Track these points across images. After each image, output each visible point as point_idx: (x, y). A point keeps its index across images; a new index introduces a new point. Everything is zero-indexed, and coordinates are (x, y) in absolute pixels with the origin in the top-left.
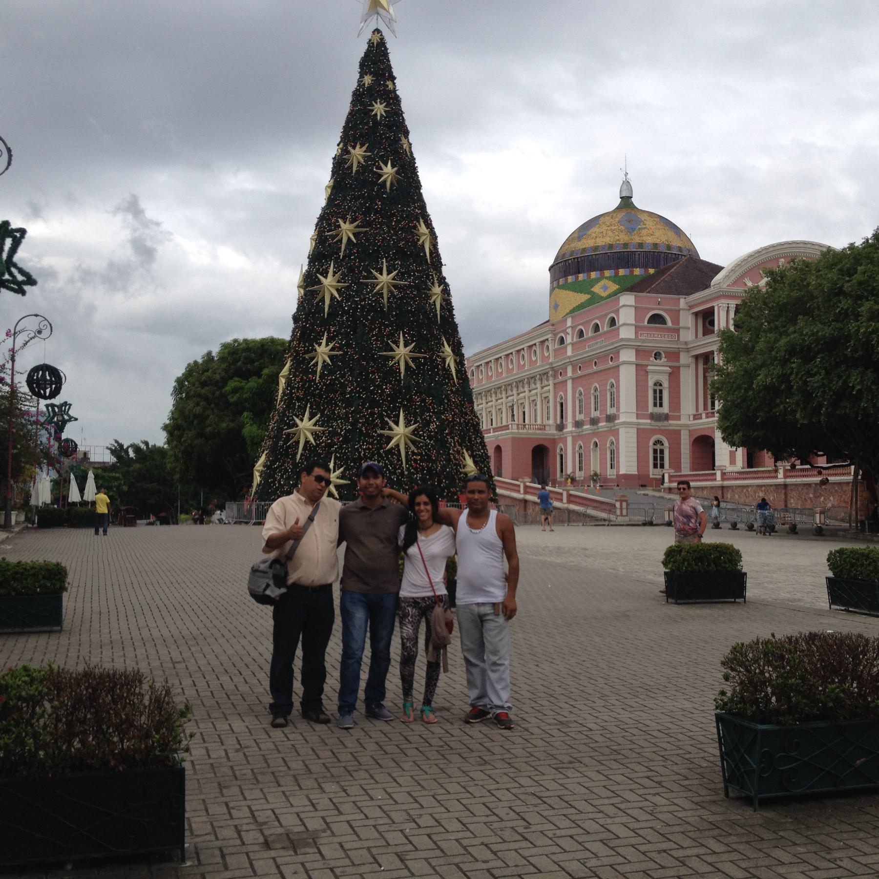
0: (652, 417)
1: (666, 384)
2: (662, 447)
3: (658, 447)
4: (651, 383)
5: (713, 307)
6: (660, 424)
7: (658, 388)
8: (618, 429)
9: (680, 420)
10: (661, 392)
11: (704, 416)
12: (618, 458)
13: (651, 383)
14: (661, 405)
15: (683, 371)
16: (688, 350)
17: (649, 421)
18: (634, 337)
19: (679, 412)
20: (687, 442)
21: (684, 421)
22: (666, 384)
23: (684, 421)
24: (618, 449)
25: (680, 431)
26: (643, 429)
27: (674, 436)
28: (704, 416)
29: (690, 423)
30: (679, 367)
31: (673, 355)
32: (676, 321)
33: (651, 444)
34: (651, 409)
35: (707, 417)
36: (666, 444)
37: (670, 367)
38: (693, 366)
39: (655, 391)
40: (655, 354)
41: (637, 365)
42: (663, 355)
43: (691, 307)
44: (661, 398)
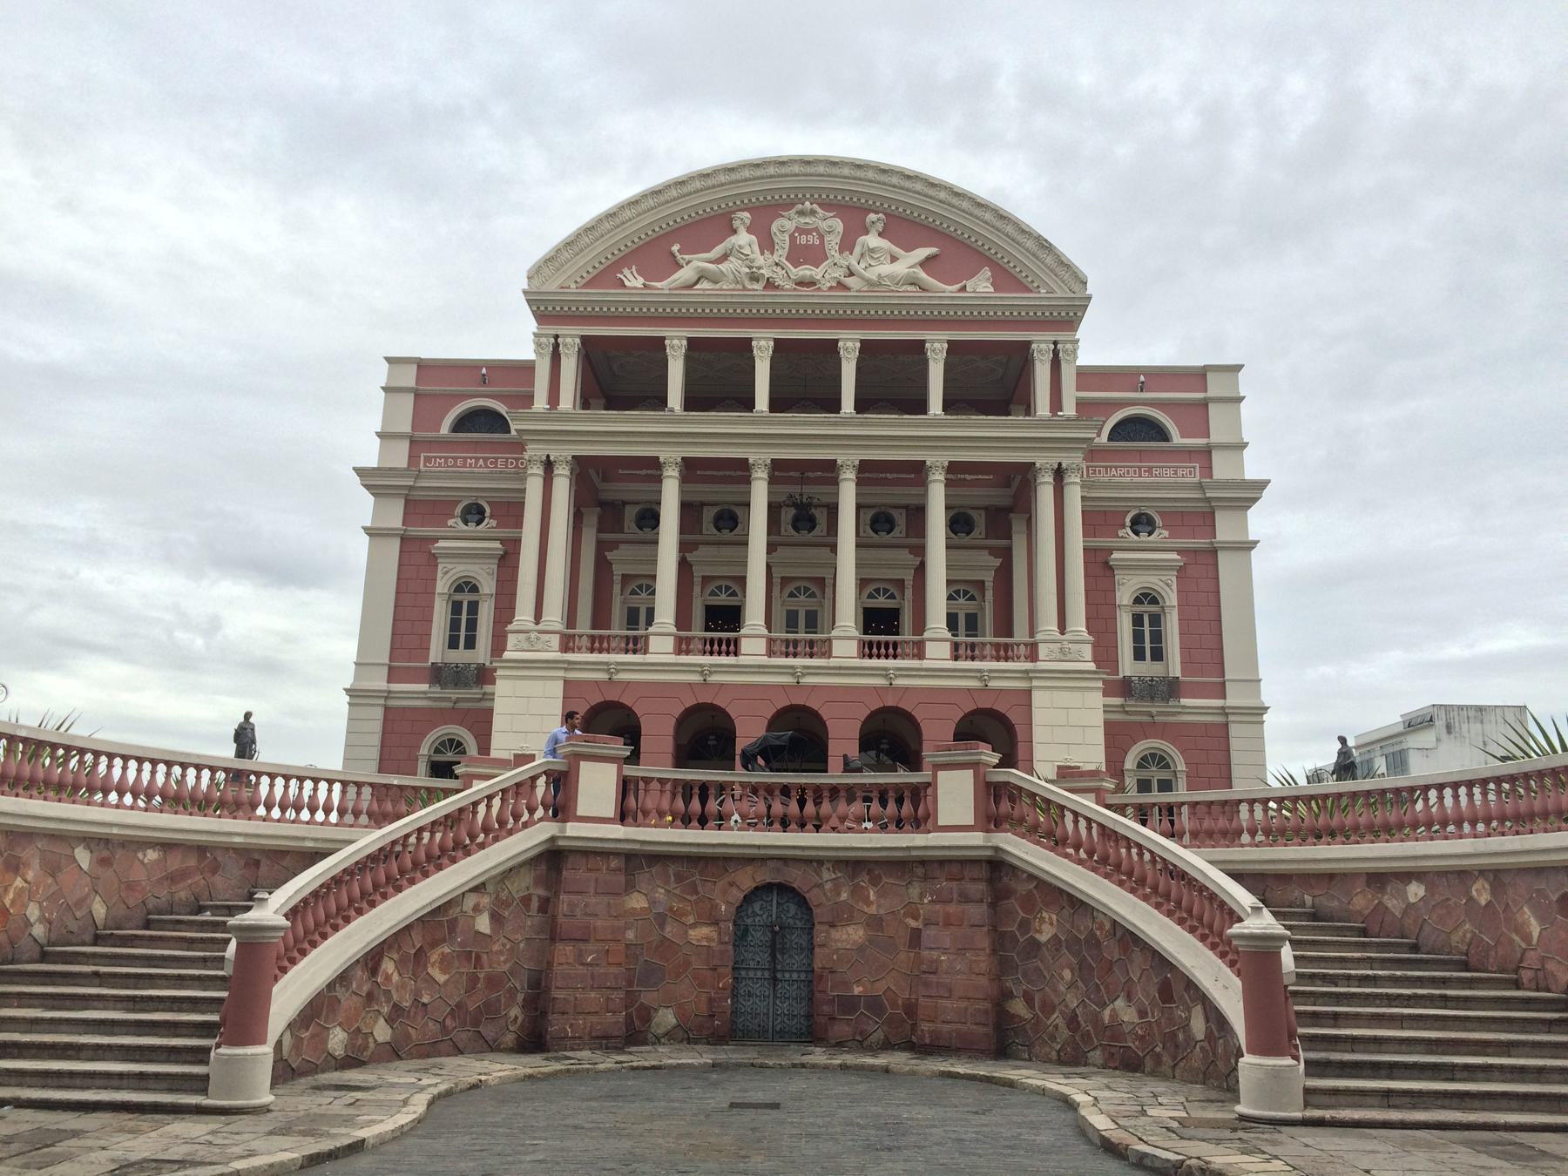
0: (438, 675)
1: (488, 586)
4: (442, 586)
6: (454, 693)
7: (466, 598)
10: (474, 607)
13: (442, 586)
14: (471, 643)
17: (425, 687)
18: (401, 461)
33: (425, 749)
34: (437, 651)
37: (502, 541)
39: (456, 607)
41: (405, 540)
42: (488, 513)
44: (472, 625)
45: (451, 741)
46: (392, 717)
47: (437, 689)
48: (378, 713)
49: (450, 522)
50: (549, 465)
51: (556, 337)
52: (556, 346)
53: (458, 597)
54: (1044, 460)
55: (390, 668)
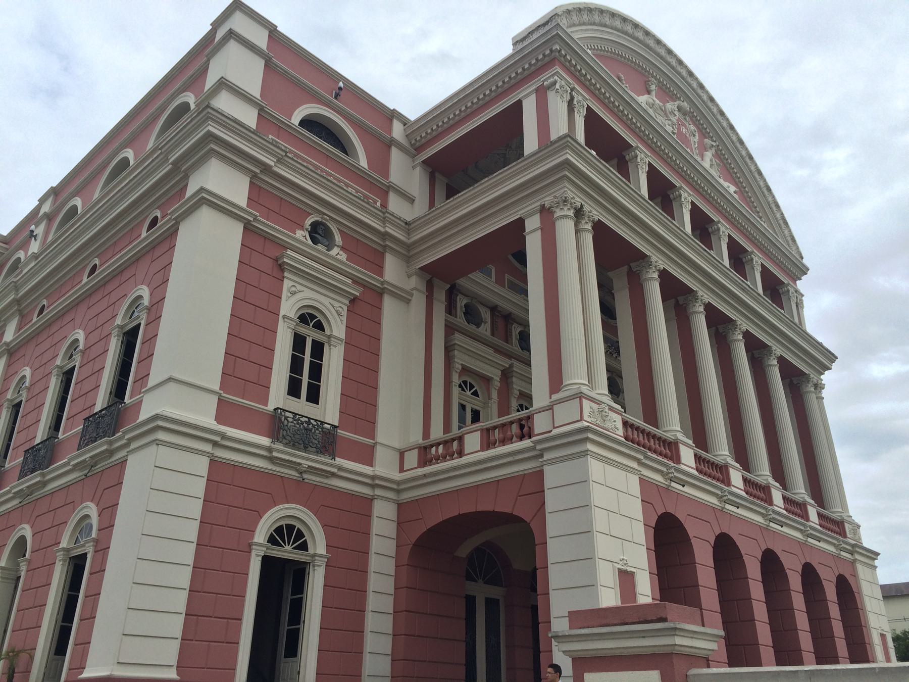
1: (337, 328)
2: (298, 556)
3: (287, 552)
4: (289, 307)
5: (517, 107)
6: (306, 459)
7: (311, 334)
8: (123, 463)
9: (370, 462)
10: (318, 349)
11: (472, 441)
12: (94, 595)
13: (289, 307)
14: (314, 396)
15: (388, 304)
16: (407, 253)
17: (265, 441)
19: (373, 437)
20: (390, 547)
21: (384, 466)
22: (337, 328)
23: (384, 466)
24: (102, 549)
25: (370, 501)
26: (235, 467)
27: (348, 517)
28: (472, 441)
29: (397, 476)
30: (380, 293)
31: (368, 251)
32: (381, 163)
33: (261, 536)
35: (487, 444)
36: (319, 545)
37: (354, 282)
38: (419, 301)
39: (299, 342)
40: (315, 226)
41: (249, 229)
42: (338, 239)
43: (419, 149)
44: (316, 372)
45: (291, 528)
46: (220, 476)
47: (280, 446)
48: (202, 466)
49: (300, 234)
50: (579, 213)
51: (572, 90)
52: (572, 98)
53: (303, 330)
54: (813, 376)
55: (221, 401)
